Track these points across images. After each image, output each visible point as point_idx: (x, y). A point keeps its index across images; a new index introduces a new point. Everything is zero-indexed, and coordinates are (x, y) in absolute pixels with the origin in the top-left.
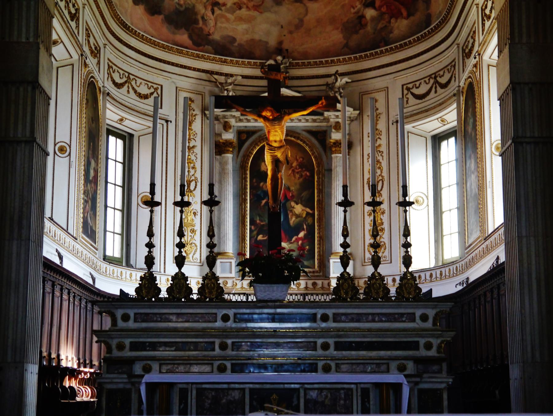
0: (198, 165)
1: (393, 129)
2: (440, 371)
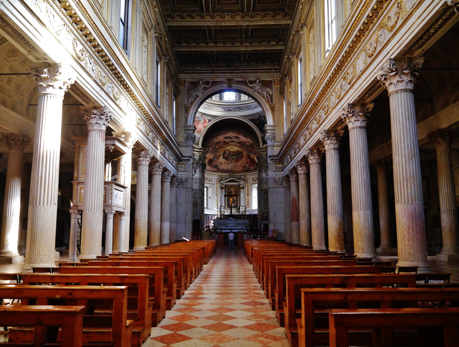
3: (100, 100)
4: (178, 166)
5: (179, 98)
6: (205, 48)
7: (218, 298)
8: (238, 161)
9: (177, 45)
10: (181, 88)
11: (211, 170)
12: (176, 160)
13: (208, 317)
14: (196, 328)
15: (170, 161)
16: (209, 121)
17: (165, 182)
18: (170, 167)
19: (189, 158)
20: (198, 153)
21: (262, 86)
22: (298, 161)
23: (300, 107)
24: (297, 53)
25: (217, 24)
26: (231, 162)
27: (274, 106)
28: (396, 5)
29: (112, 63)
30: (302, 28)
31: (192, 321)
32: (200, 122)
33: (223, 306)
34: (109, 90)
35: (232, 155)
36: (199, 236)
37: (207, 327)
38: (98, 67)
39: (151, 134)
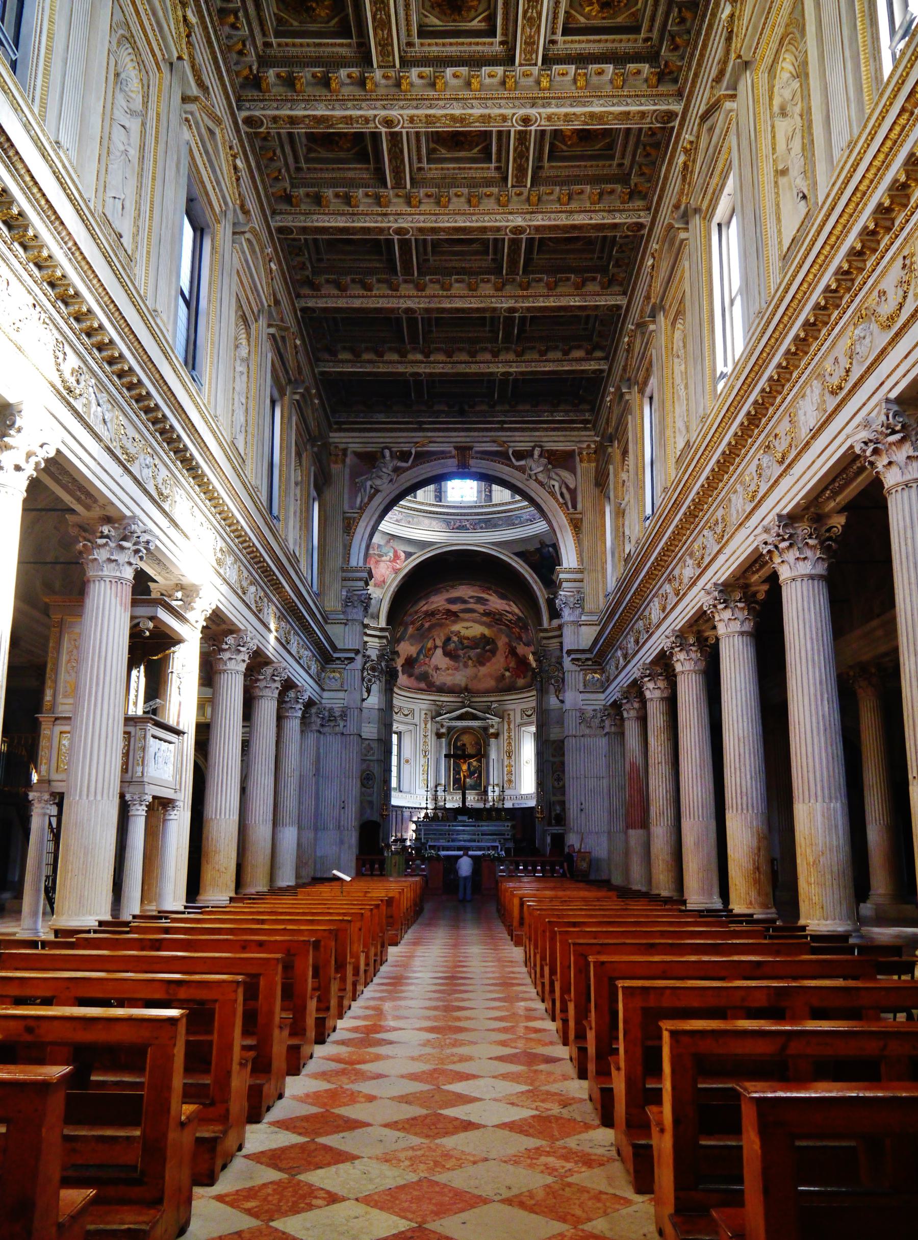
3: (120, 499)
4: (323, 674)
5: (328, 494)
6: (399, 366)
7: (429, 1041)
8: (482, 664)
9: (326, 356)
10: (335, 468)
11: (410, 685)
12: (317, 660)
13: (402, 1096)
14: (369, 1129)
15: (301, 662)
16: (408, 555)
17: (287, 717)
18: (302, 679)
19: (352, 655)
20: (377, 640)
21: (550, 466)
22: (644, 664)
23: (649, 521)
24: (640, 380)
25: (433, 305)
26: (466, 665)
27: (582, 519)
28: (899, 262)
29: (156, 405)
30: (653, 315)
31: (358, 1106)
32: (384, 558)
33: (442, 1063)
34: (145, 475)
36: (377, 866)
37: (400, 1126)
38: (118, 413)
39: (252, 589)
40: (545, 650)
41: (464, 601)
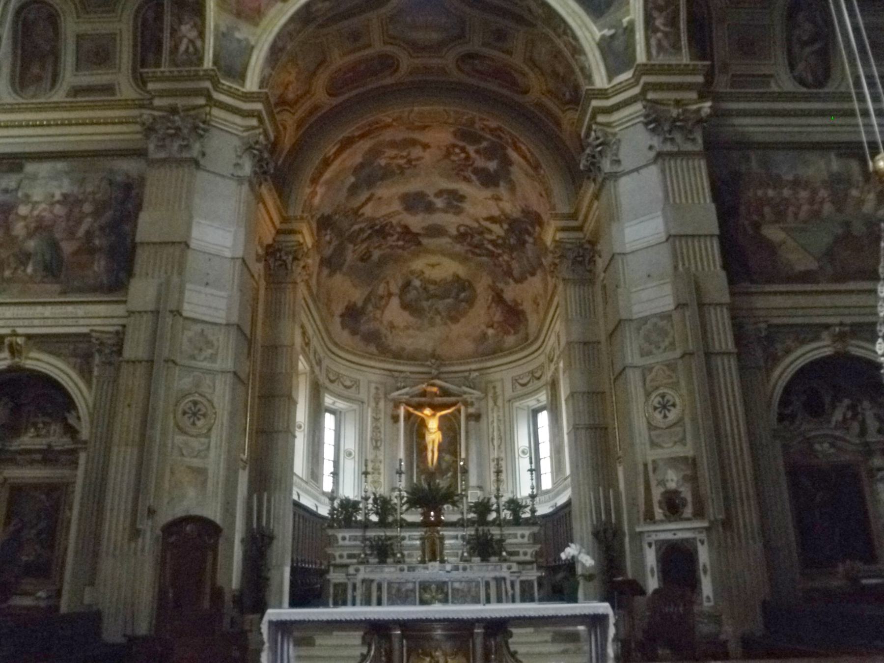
0: (383, 431)
1: (507, 405)
2: (532, 569)
8: (455, 320)
26: (432, 324)
35: (434, 296)
40: (606, 134)
41: (430, 208)
